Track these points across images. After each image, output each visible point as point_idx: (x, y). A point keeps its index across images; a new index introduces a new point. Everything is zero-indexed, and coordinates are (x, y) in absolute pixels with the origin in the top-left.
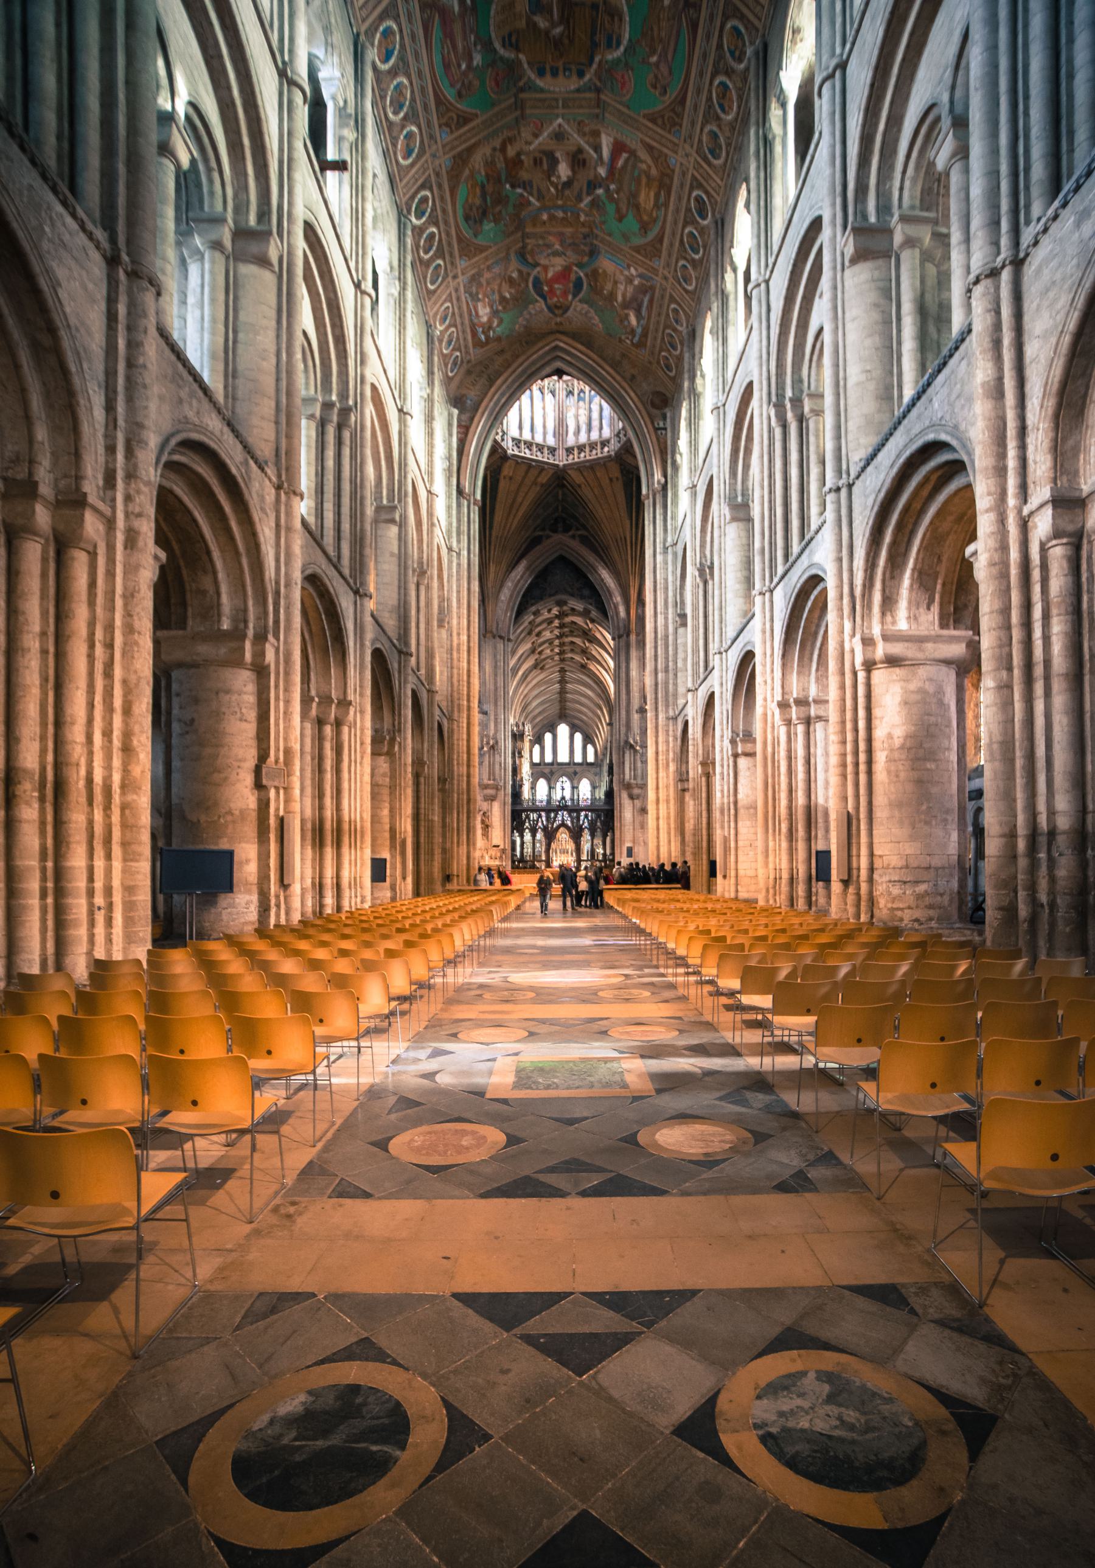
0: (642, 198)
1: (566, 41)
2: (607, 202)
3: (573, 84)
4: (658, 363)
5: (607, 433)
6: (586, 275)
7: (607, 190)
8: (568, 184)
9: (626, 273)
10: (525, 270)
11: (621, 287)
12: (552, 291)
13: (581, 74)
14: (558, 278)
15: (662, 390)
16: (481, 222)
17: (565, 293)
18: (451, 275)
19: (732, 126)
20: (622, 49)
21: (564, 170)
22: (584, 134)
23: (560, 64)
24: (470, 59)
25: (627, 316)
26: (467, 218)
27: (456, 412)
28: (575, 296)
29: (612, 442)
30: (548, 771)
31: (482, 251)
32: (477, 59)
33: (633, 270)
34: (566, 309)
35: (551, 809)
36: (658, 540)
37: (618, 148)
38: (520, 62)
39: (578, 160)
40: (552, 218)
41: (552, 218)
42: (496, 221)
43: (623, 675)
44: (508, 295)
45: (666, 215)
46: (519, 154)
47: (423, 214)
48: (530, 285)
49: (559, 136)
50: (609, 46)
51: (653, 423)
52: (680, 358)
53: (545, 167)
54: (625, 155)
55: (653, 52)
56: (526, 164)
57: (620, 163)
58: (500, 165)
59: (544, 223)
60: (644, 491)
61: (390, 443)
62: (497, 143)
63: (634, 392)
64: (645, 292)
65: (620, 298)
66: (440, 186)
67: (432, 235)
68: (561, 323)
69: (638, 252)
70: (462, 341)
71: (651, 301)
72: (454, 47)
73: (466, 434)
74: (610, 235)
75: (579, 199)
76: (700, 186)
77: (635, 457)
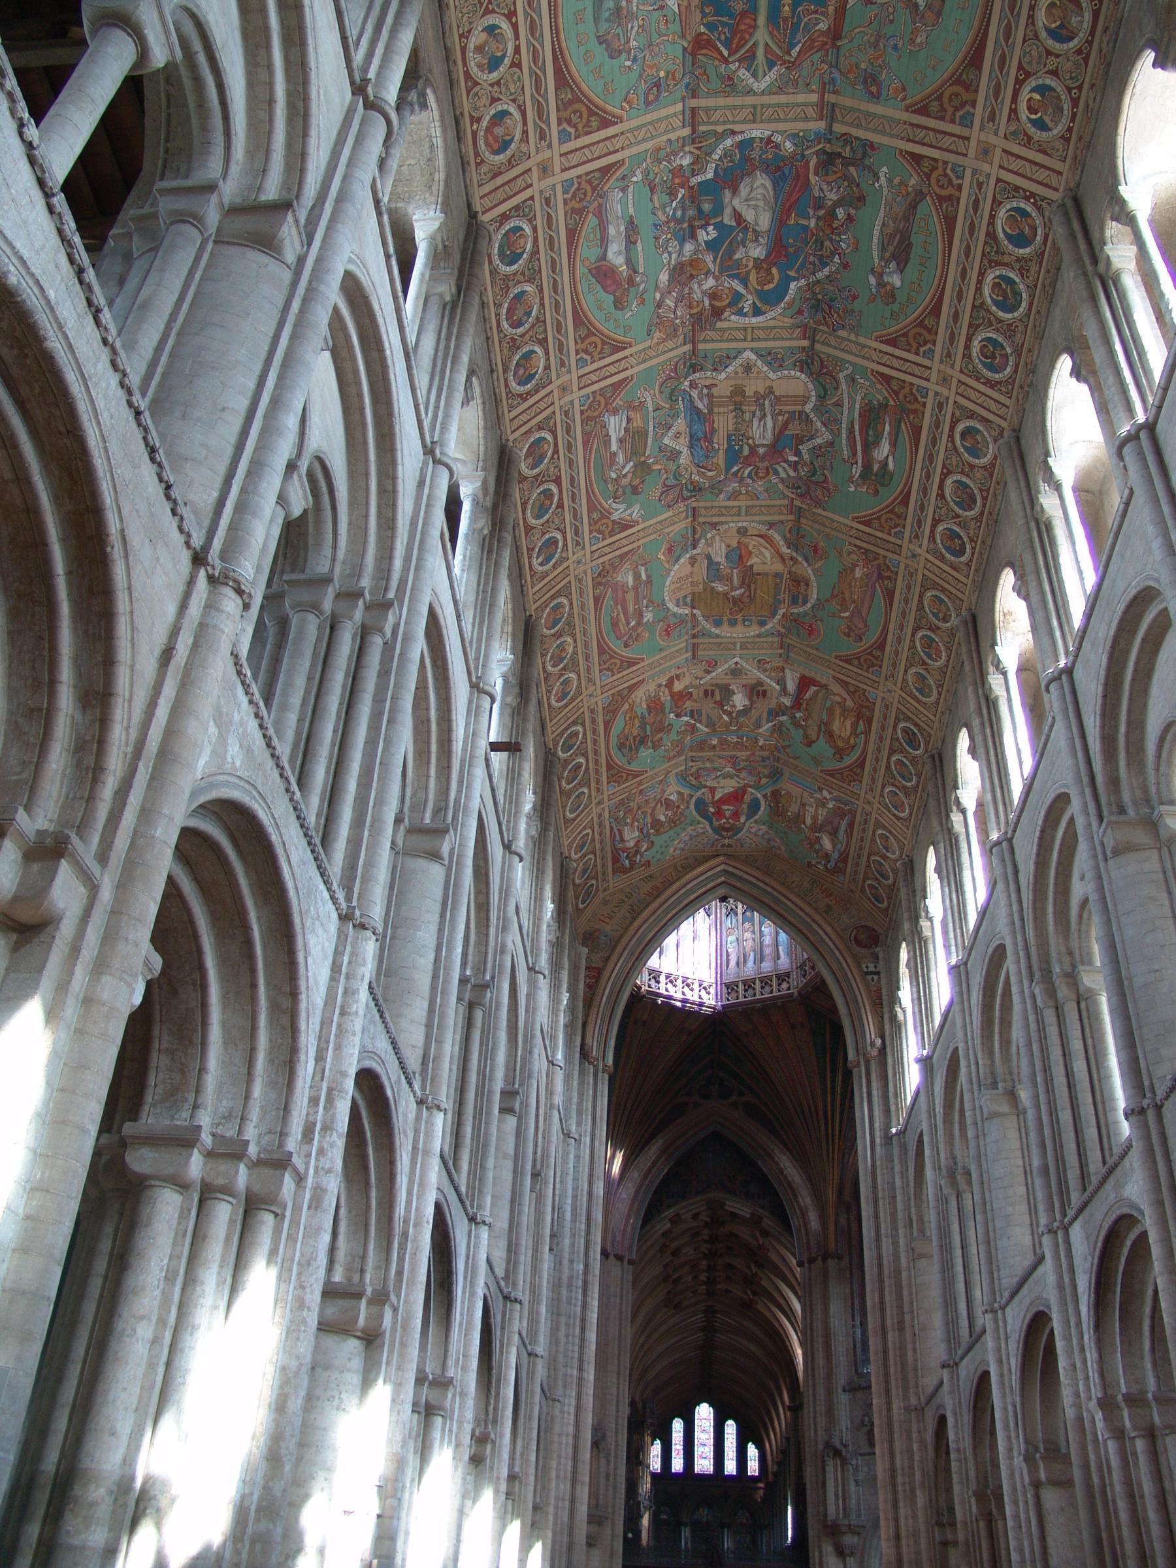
0: (836, 726)
1: (746, 600)
2: (792, 728)
3: (753, 631)
4: (863, 890)
5: (784, 962)
6: (765, 796)
8: (746, 711)
9: (817, 796)
10: (686, 791)
11: (810, 811)
12: (719, 813)
13: (762, 623)
14: (727, 799)
15: (870, 923)
16: (637, 750)
17: (736, 815)
18: (595, 802)
19: (943, 671)
20: (809, 605)
21: (739, 701)
22: (765, 670)
23: (739, 617)
24: (641, 616)
25: (818, 840)
26: (621, 747)
27: (585, 950)
28: (749, 817)
29: (794, 975)
31: (636, 776)
32: (648, 617)
33: (825, 793)
34: (736, 830)
37: (805, 683)
38: (694, 616)
39: (756, 692)
40: (723, 742)
41: (723, 742)
42: (655, 747)
43: (818, 1325)
44: (663, 818)
45: (866, 743)
46: (686, 687)
47: (571, 747)
48: (692, 806)
49: (736, 672)
50: (794, 601)
51: (859, 967)
52: (893, 890)
54: (813, 689)
56: (695, 696)
57: (808, 695)
58: (666, 698)
59: (714, 747)
61: (516, 1010)
65: (809, 821)
66: (593, 721)
67: (579, 766)
68: (730, 846)
69: (832, 776)
70: (599, 868)
71: (851, 825)
73: (598, 978)
74: (796, 758)
75: (758, 725)
76: (907, 719)
77: (830, 996)
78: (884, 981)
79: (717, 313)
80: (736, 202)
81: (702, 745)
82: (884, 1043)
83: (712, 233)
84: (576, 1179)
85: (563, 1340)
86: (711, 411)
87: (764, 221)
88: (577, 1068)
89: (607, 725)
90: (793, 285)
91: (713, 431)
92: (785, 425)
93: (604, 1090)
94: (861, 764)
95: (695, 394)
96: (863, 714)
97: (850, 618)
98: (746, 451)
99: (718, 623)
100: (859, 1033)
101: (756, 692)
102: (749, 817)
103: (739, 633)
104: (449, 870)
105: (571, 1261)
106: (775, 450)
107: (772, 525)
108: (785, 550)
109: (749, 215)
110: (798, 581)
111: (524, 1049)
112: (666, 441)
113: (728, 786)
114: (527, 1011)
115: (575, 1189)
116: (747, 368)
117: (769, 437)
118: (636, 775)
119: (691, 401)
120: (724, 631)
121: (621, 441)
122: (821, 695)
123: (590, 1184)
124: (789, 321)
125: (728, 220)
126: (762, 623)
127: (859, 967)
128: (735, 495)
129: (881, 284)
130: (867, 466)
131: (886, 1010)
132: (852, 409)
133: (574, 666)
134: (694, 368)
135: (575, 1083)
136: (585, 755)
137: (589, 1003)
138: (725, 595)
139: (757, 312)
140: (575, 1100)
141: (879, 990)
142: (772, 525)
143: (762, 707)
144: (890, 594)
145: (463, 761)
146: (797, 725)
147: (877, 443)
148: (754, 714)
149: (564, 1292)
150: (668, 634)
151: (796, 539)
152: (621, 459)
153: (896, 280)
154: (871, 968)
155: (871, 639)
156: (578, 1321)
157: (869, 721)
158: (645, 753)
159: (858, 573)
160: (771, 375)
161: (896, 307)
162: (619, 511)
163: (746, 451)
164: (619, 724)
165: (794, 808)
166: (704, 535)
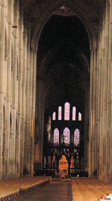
30: (61, 125)
35: (62, 146)
82: (97, 47)
84: (30, 78)
85: (28, 112)
88: (29, 53)
93: (36, 56)
104: (8, 61)
105: (30, 95)
111: (19, 67)
114: (19, 59)
115: (30, 80)
123: (33, 78)
127: (93, 27)
135: (29, 56)
137: (31, 37)
140: (29, 60)
145: (8, 40)
149: (28, 102)
154: (96, 28)
156: (31, 107)
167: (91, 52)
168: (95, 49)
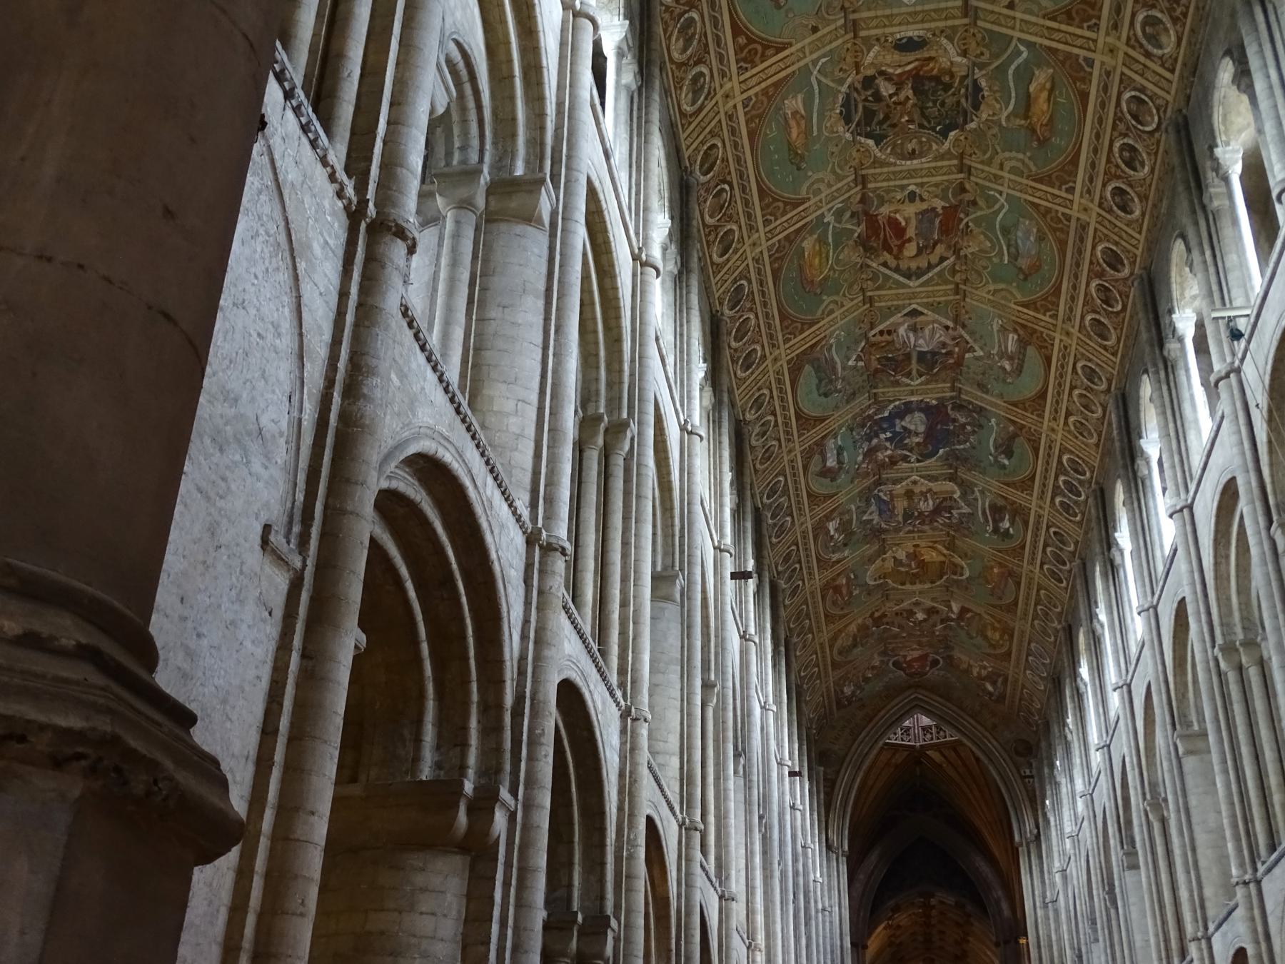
0: (989, 633)
3: (928, 586)
7: (959, 625)
8: (925, 620)
10: (886, 659)
20: (964, 577)
24: (851, 593)
26: (840, 653)
28: (931, 668)
32: (856, 592)
36: (1036, 893)
37: (964, 610)
42: (862, 646)
48: (891, 664)
49: (917, 604)
50: (955, 573)
51: (1019, 771)
53: (905, 615)
55: (989, 584)
57: (969, 615)
58: (869, 622)
60: (1017, 838)
62: (868, 615)
63: (997, 740)
64: (1000, 675)
72: (841, 594)
78: (1037, 785)
79: (893, 462)
80: (903, 423)
81: (895, 636)
83: (889, 435)
86: (892, 499)
87: (922, 429)
89: (831, 647)
90: (941, 451)
91: (894, 508)
92: (942, 502)
94: (1009, 654)
95: (881, 494)
96: (1008, 632)
97: (994, 588)
98: (916, 514)
99: (903, 584)
100: (1021, 823)
101: (931, 612)
102: (931, 668)
103: (918, 587)
106: (937, 511)
107: (935, 542)
108: (945, 552)
109: (912, 427)
110: (955, 565)
112: (865, 518)
113: (916, 654)
116: (915, 483)
117: (931, 507)
118: (850, 662)
119: (879, 497)
120: (908, 587)
121: (836, 530)
122: (977, 617)
124: (939, 464)
125: (898, 429)
126: (932, 582)
127: (1019, 771)
128: (909, 532)
129: (996, 461)
130: (996, 530)
131: (1039, 807)
132: (983, 504)
133: (811, 630)
134: (880, 485)
136: (818, 666)
138: (907, 572)
139: (918, 461)
141: (1034, 791)
142: (935, 542)
143: (935, 618)
144: (1018, 584)
146: (962, 628)
147: (1002, 519)
148: (931, 621)
150: (869, 594)
151: (951, 546)
152: (837, 536)
153: (1006, 462)
154: (1028, 773)
155: (1008, 599)
157: (1012, 636)
158: (859, 650)
159: (996, 570)
160: (931, 484)
161: (1007, 471)
162: (835, 557)
163: (916, 514)
164: (839, 642)
165: (965, 666)
166: (891, 548)
167: (1020, 849)
168: (1033, 838)
